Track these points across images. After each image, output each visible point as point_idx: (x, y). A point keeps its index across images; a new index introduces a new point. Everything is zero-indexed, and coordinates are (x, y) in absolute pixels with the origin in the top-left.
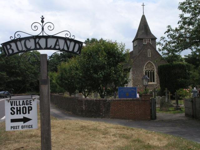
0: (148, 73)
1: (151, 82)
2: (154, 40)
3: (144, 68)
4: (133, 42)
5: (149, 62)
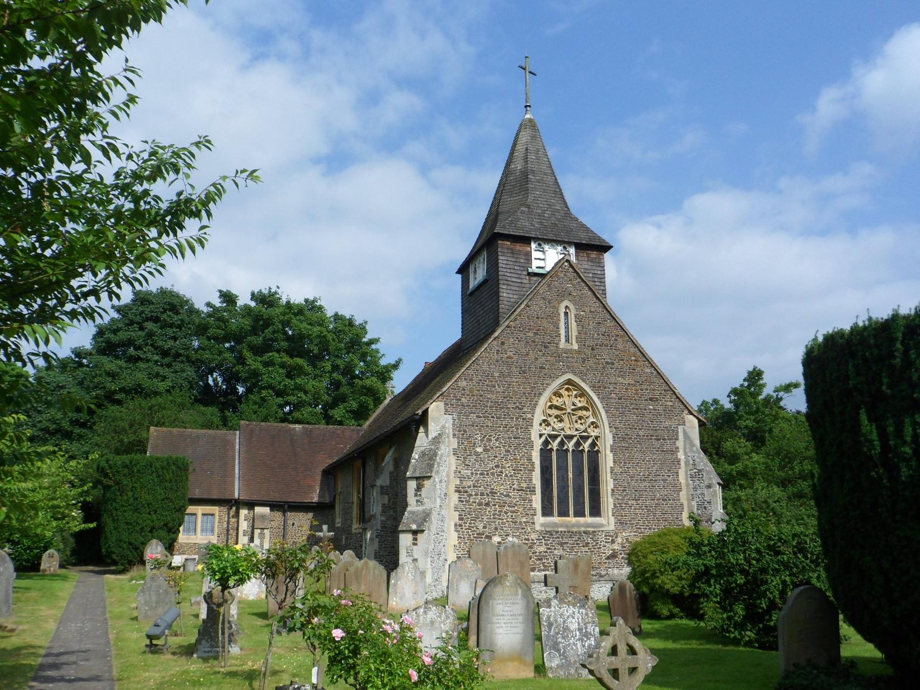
0: (562, 452)
1: (579, 513)
2: (594, 254)
3: (539, 416)
4: (464, 270)
5: (569, 382)
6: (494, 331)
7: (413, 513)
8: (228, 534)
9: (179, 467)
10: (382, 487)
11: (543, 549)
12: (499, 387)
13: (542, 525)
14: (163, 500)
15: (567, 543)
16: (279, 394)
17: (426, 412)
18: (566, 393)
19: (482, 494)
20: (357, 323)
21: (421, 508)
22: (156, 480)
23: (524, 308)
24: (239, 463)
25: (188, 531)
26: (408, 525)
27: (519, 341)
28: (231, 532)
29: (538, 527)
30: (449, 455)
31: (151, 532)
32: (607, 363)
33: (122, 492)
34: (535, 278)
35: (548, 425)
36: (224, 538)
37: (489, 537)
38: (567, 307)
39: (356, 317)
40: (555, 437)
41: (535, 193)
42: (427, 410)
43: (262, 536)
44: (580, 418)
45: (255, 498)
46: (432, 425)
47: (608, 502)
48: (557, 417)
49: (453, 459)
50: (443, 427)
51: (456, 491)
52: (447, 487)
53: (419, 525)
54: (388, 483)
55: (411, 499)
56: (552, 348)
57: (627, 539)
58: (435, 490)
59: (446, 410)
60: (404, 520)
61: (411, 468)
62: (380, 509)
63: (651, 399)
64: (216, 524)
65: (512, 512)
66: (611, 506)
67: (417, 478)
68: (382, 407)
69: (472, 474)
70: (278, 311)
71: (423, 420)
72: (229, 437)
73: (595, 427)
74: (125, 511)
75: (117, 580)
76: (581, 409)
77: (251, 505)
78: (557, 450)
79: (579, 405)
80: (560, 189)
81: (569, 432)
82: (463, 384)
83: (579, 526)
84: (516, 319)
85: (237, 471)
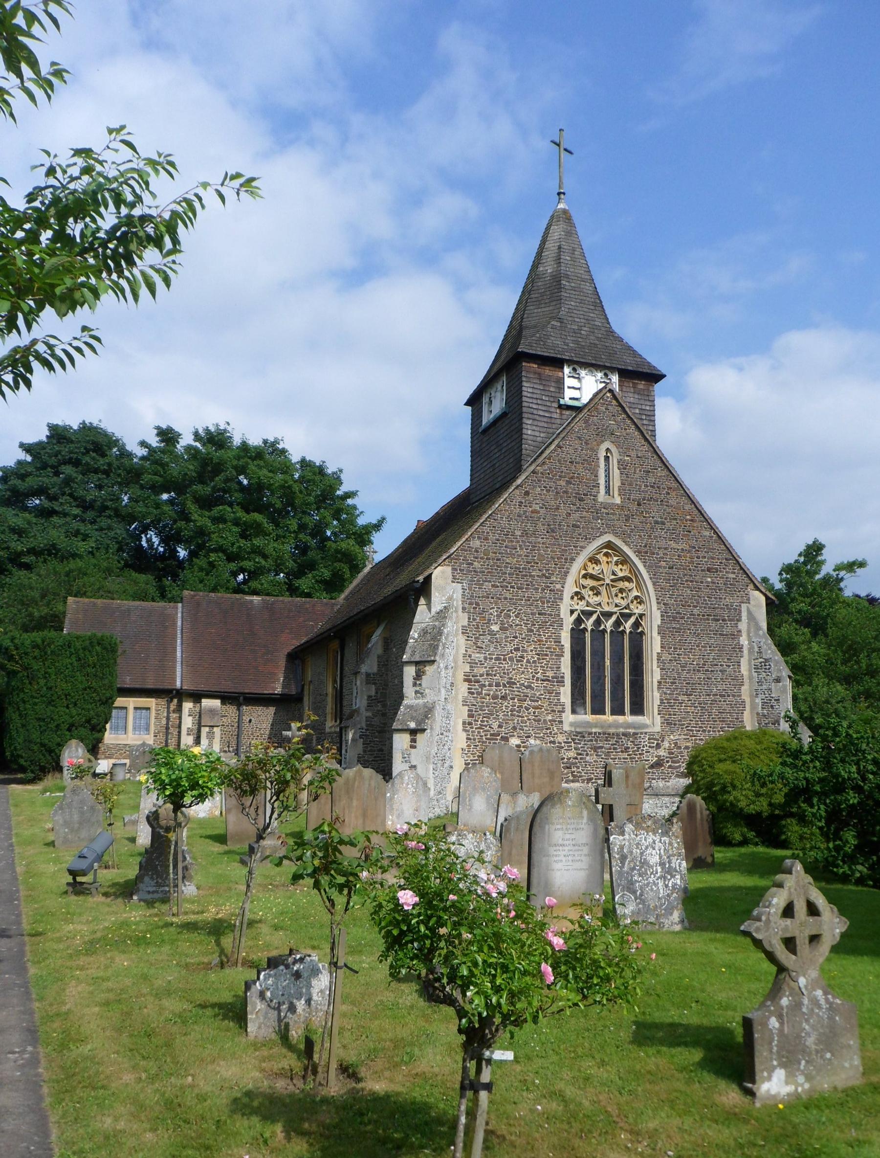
0: (598, 634)
1: (618, 710)
2: (641, 385)
3: (570, 588)
4: (475, 401)
5: (609, 545)
6: (515, 478)
7: (410, 707)
8: (167, 733)
9: (105, 648)
10: (368, 675)
11: (572, 754)
12: (521, 549)
13: (571, 724)
14: (85, 689)
15: (602, 747)
16: (230, 558)
17: (428, 579)
18: (605, 558)
19: (498, 685)
20: (329, 471)
21: (420, 701)
22: (76, 664)
23: (555, 450)
24: (182, 644)
25: (116, 729)
26: (404, 722)
27: (548, 491)
28: (171, 730)
29: (566, 727)
30: (456, 635)
31: (69, 730)
32: (657, 522)
33: (32, 679)
34: (568, 413)
35: (582, 598)
36: (162, 738)
37: (506, 739)
38: (608, 450)
39: (327, 464)
40: (590, 614)
41: (569, 304)
42: (430, 576)
43: (211, 736)
44: (621, 591)
45: (202, 687)
46: (436, 596)
47: (653, 697)
48: (592, 589)
49: (462, 640)
50: (451, 598)
51: (465, 680)
52: (454, 676)
53: (419, 723)
54: (375, 669)
55: (409, 690)
56: (588, 501)
57: (676, 744)
58: (439, 678)
59: (454, 577)
60: (400, 716)
61: (408, 650)
62: (365, 702)
63: (709, 570)
64: (153, 720)
65: (536, 708)
66: (657, 702)
67: (417, 663)
68: (361, 576)
69: (485, 658)
70: (230, 454)
71: (424, 589)
72: (169, 611)
73: (640, 603)
74: (35, 704)
75: (27, 791)
76: (622, 579)
77: (197, 697)
78: (592, 630)
79: (621, 574)
80: (601, 302)
81: (607, 609)
82: (476, 543)
83: (617, 725)
84: (544, 463)
85: (179, 654)
